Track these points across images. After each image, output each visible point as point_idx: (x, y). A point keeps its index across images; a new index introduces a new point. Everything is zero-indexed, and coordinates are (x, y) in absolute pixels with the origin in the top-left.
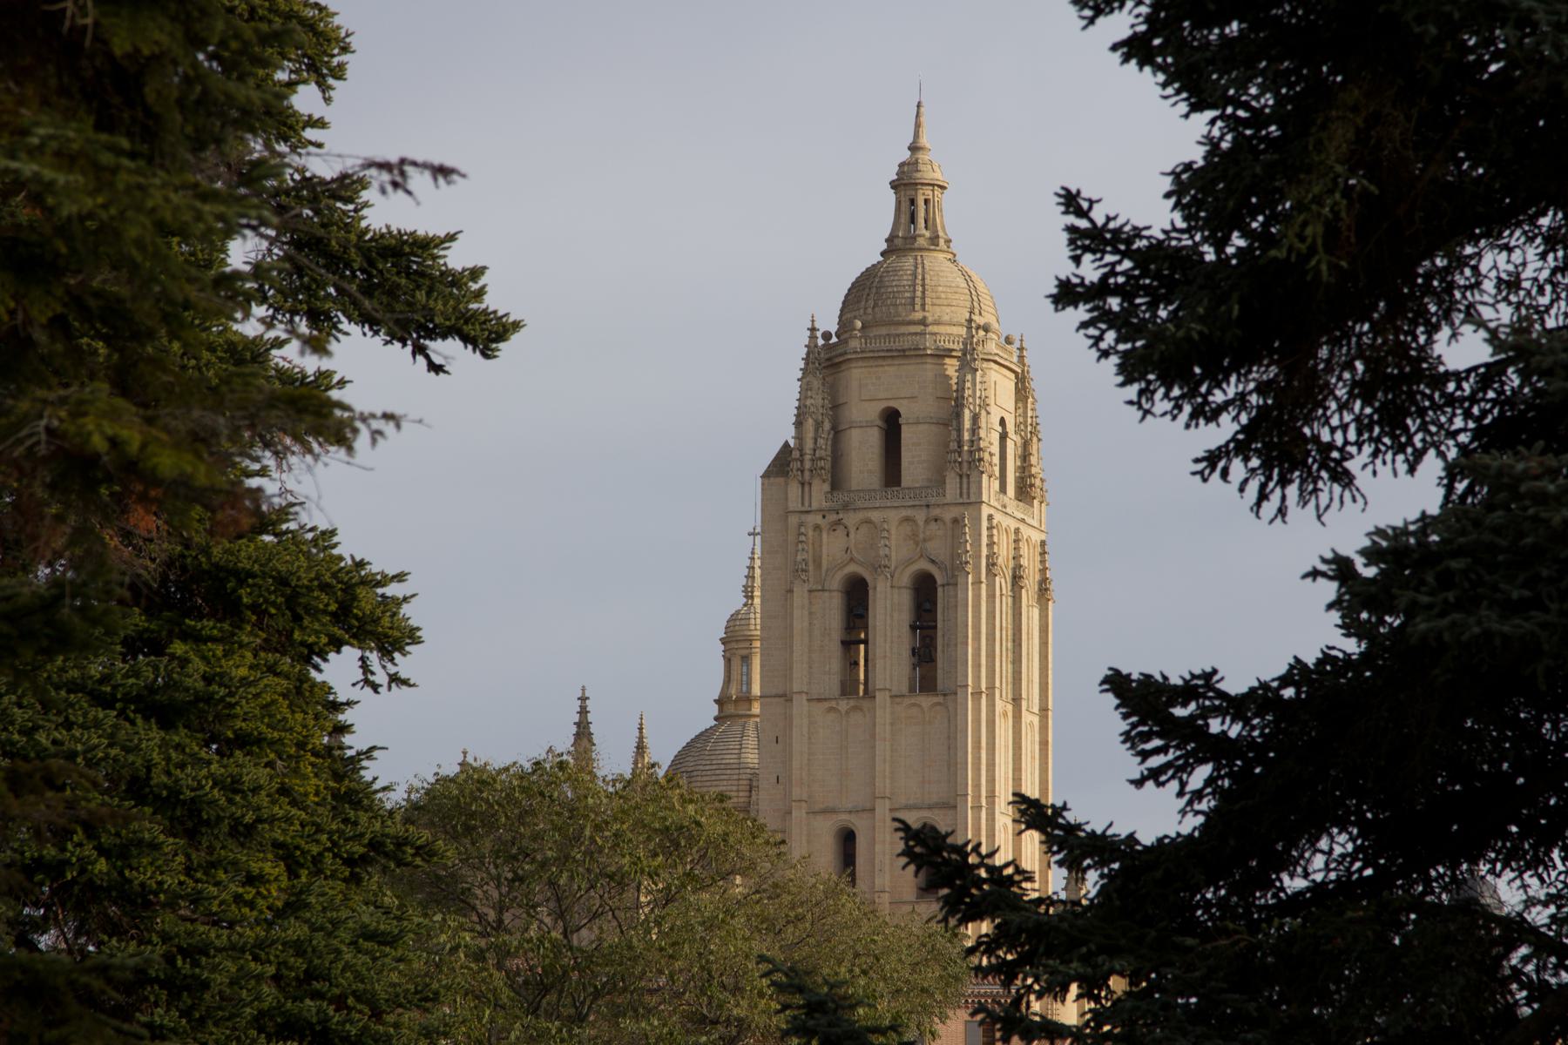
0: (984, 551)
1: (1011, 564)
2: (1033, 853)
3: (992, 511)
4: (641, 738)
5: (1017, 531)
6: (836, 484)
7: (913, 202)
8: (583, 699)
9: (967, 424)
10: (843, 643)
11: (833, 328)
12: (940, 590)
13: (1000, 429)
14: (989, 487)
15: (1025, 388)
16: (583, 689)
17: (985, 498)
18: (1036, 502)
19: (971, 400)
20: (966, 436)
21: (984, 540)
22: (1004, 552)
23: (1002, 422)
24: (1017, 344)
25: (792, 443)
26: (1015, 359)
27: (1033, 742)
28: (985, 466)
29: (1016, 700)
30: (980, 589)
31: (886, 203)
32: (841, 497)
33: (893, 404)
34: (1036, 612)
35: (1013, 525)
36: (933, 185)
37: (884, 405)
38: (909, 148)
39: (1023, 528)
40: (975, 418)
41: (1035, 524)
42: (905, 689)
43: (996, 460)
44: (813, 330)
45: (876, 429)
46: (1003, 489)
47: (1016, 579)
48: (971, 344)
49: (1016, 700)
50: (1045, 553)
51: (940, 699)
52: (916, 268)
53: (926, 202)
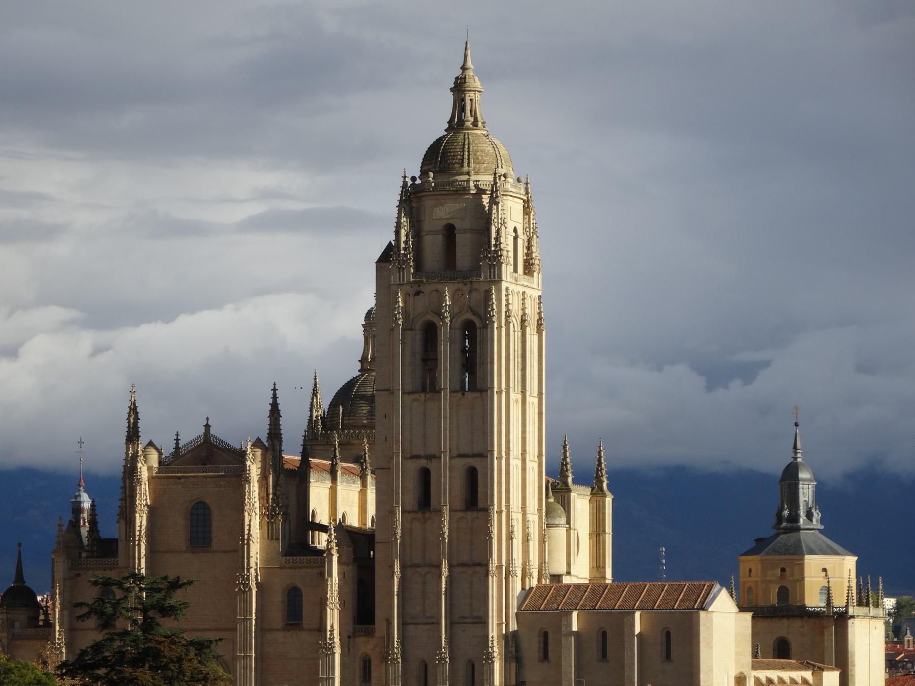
0: (504, 309)
1: (520, 313)
2: (534, 478)
3: (508, 285)
5: (524, 293)
7: (463, 100)
8: (275, 390)
9: (494, 235)
10: (422, 360)
11: (417, 174)
12: (478, 331)
13: (514, 234)
14: (507, 270)
15: (528, 207)
16: (275, 384)
17: (504, 278)
18: (535, 274)
19: (496, 220)
20: (493, 242)
21: (504, 302)
22: (515, 308)
23: (515, 230)
25: (393, 243)
26: (523, 192)
27: (534, 413)
28: (504, 259)
29: (523, 392)
30: (501, 331)
31: (449, 98)
33: (452, 221)
34: (536, 338)
35: (521, 289)
36: (475, 91)
37: (445, 222)
38: (461, 68)
39: (527, 290)
40: (498, 232)
41: (535, 286)
42: (458, 387)
43: (511, 254)
44: (405, 177)
45: (441, 236)
46: (515, 270)
47: (523, 321)
48: (496, 188)
49: (523, 392)
50: (541, 303)
52: (465, 141)
53: (471, 100)
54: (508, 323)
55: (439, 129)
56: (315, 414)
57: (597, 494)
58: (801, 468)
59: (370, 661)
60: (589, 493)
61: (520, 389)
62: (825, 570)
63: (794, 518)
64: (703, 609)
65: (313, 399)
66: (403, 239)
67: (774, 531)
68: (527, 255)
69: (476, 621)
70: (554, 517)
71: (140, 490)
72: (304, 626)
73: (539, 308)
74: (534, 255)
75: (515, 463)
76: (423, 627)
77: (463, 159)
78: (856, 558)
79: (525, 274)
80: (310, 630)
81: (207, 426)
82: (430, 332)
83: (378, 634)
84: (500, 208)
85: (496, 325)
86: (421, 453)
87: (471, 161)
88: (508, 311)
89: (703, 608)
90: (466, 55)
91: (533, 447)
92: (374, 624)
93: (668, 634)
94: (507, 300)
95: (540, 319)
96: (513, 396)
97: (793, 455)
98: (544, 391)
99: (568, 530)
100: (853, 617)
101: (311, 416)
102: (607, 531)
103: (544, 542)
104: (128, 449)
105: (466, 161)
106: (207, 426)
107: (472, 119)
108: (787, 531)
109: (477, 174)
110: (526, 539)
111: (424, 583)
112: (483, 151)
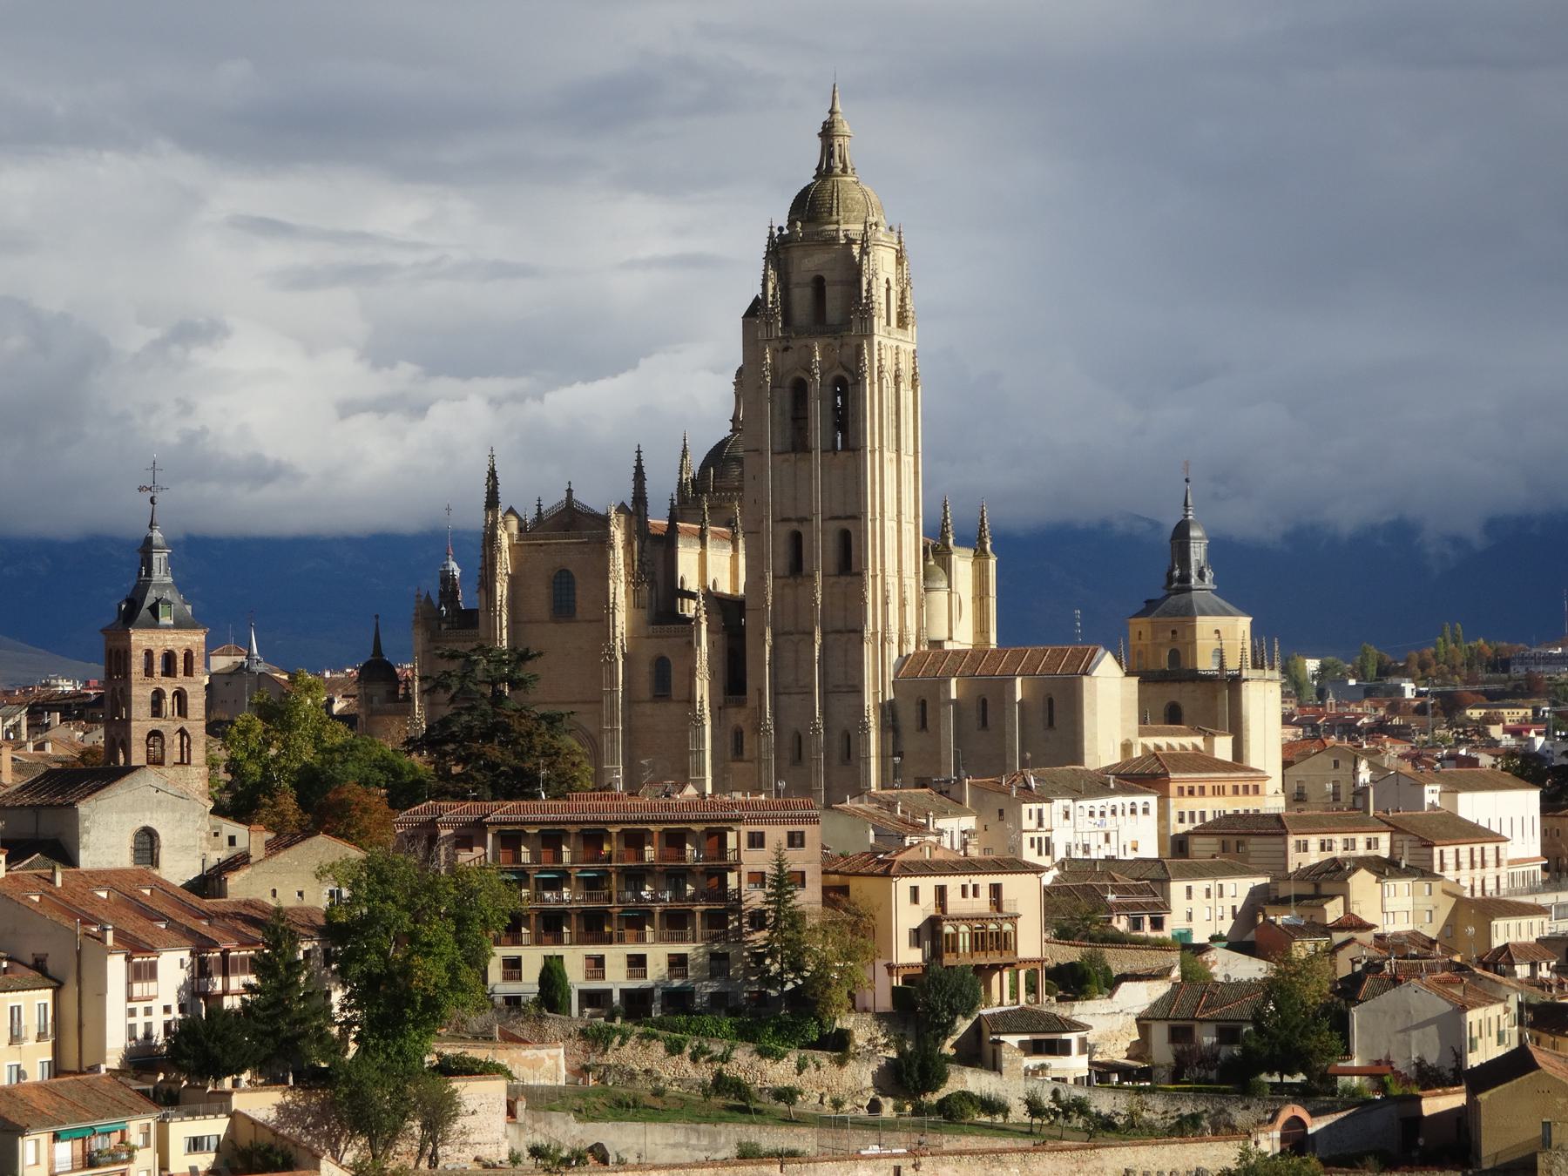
0: (876, 364)
1: (894, 368)
3: (880, 339)
4: (685, 445)
5: (897, 347)
7: (832, 145)
8: (639, 452)
9: (865, 287)
11: (785, 224)
13: (886, 286)
14: (879, 324)
15: (901, 257)
17: (876, 331)
18: (909, 327)
20: (864, 294)
21: (876, 357)
22: (888, 363)
23: (888, 281)
24: (896, 229)
25: (760, 296)
26: (895, 241)
28: (875, 312)
29: (898, 450)
31: (818, 143)
33: (819, 273)
34: (911, 394)
37: (814, 274)
39: (901, 344)
40: (869, 283)
41: (909, 340)
42: (829, 446)
43: (884, 306)
44: (771, 227)
46: (888, 323)
47: (897, 377)
49: (898, 450)
51: (851, 454)
53: (840, 145)
54: (880, 379)
55: (807, 177)
56: (685, 477)
57: (980, 555)
58: (1192, 526)
59: (742, 733)
60: (972, 555)
61: (895, 448)
62: (1217, 632)
63: (1185, 578)
64: (1086, 674)
65: (682, 461)
66: (770, 292)
67: (1165, 592)
68: (901, 307)
69: (850, 689)
70: (934, 581)
71: (501, 558)
72: (674, 698)
73: (914, 363)
74: (908, 308)
75: (890, 525)
76: (795, 696)
77: (831, 208)
78: (1250, 619)
79: (899, 327)
80: (679, 702)
81: (569, 491)
82: (800, 391)
84: (871, 258)
85: (868, 381)
86: (792, 516)
87: (841, 209)
88: (880, 366)
89: (1086, 673)
90: (834, 99)
91: (910, 508)
92: (744, 693)
93: (1051, 701)
94: (880, 355)
95: (915, 374)
96: (886, 455)
97: (1184, 512)
98: (920, 450)
100: (1247, 680)
101: (681, 479)
102: (991, 594)
103: (922, 607)
104: (487, 516)
105: (835, 210)
106: (569, 491)
107: (841, 166)
108: (1179, 591)
109: (847, 222)
110: (903, 604)
111: (797, 651)
112: (852, 199)
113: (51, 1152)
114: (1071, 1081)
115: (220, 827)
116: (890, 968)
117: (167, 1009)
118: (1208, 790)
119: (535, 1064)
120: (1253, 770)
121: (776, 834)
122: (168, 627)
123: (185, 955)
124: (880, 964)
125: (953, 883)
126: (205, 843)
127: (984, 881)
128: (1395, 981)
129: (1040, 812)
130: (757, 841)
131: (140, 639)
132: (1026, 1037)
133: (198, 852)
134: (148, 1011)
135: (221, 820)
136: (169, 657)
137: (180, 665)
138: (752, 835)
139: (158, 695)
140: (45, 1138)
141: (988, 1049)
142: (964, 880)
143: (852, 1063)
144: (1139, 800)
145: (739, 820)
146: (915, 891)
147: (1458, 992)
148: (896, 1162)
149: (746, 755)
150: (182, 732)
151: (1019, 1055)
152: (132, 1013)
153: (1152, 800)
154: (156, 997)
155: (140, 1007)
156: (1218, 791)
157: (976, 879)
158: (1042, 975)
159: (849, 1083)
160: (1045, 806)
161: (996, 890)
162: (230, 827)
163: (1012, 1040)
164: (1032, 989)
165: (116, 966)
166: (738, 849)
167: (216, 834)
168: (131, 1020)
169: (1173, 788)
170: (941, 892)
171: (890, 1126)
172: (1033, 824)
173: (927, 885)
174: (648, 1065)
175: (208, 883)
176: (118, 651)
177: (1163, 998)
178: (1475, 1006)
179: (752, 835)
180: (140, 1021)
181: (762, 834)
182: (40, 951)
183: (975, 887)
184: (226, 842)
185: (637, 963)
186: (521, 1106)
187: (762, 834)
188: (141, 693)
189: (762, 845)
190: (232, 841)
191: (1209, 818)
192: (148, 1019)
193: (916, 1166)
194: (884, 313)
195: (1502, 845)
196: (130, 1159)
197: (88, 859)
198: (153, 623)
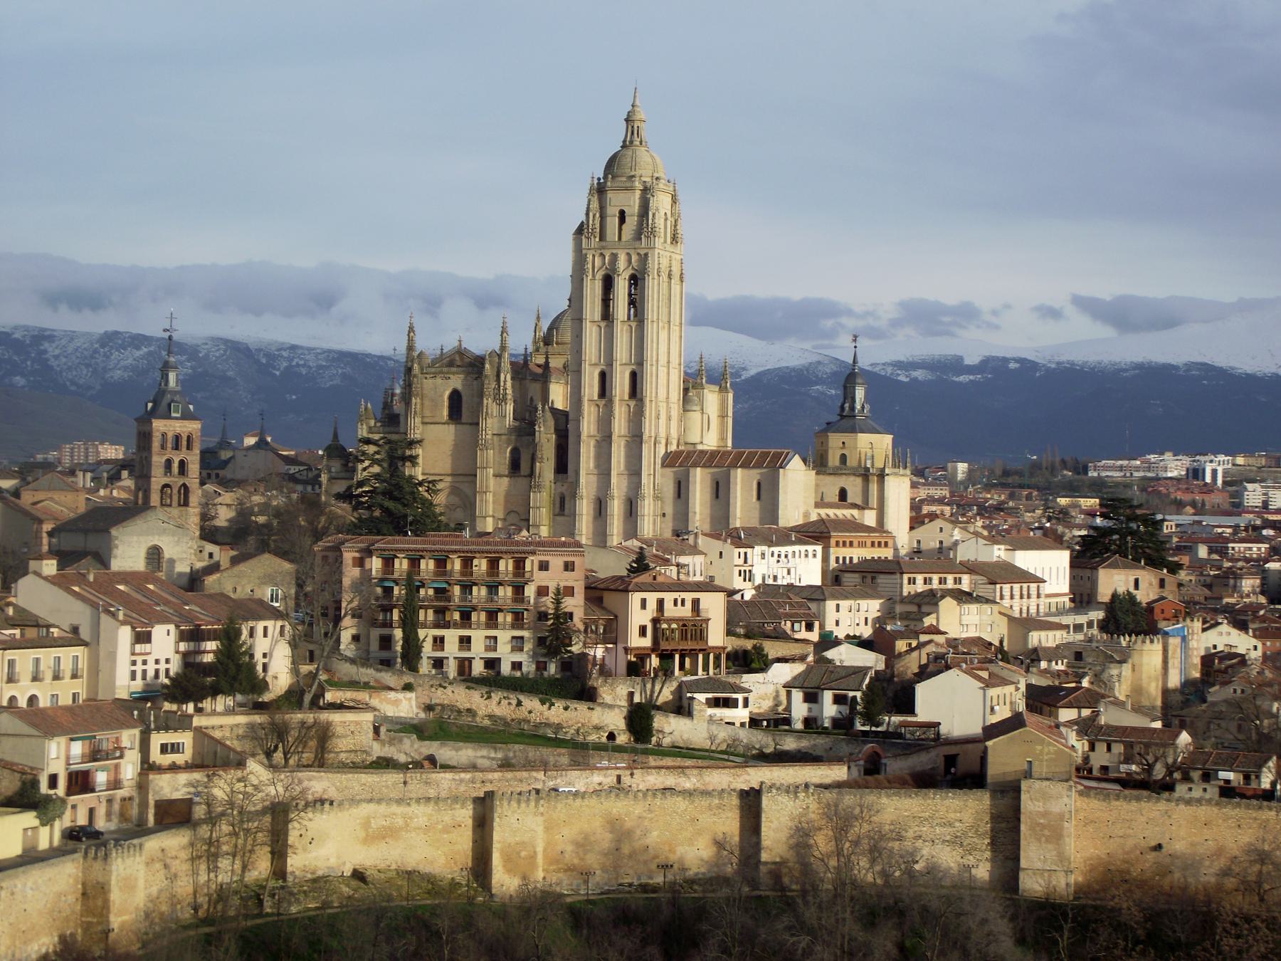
6: (602, 237)
11: (601, 176)
14: (659, 242)
21: (656, 262)
26: (672, 189)
29: (669, 322)
32: (603, 244)
34: (678, 287)
35: (668, 254)
40: (654, 215)
43: (662, 231)
46: (665, 242)
47: (670, 276)
57: (723, 390)
63: (852, 408)
82: (608, 283)
83: (570, 480)
90: (635, 97)
92: (566, 473)
99: (703, 413)
110: (669, 418)
113: (68, 749)
114: (738, 724)
115: (203, 547)
116: (626, 650)
117: (157, 662)
118: (855, 543)
119: (396, 703)
120: (885, 532)
121: (556, 562)
122: (176, 418)
123: (172, 627)
124: (620, 646)
125: (669, 597)
126: (193, 557)
127: (689, 597)
128: (948, 668)
129: (746, 553)
130: (544, 566)
131: (159, 425)
132: (710, 695)
133: (189, 562)
134: (145, 663)
135: (204, 543)
136: (177, 438)
137: (184, 443)
138: (541, 562)
139: (169, 463)
140: (63, 740)
141: (685, 703)
142: (676, 595)
143: (598, 709)
144: (810, 548)
145: (533, 553)
146: (644, 604)
147: (985, 674)
148: (618, 772)
149: (566, 511)
150: (184, 485)
151: (704, 707)
152: (134, 663)
153: (819, 549)
154: (150, 653)
155: (139, 659)
156: (862, 545)
157: (684, 595)
158: (723, 657)
159: (595, 721)
160: (749, 551)
161: (696, 603)
162: (210, 547)
163: (701, 697)
164: (717, 666)
165: (125, 634)
166: (532, 571)
167: (201, 551)
168: (133, 668)
169: (833, 542)
170: (661, 603)
171: (620, 749)
172: (741, 561)
173: (652, 598)
174: (468, 706)
175: (194, 582)
176: (144, 433)
177: (799, 675)
178: (994, 686)
179: (541, 562)
180: (139, 668)
181: (548, 562)
182: (76, 622)
183: (683, 601)
184: (207, 556)
185: (465, 642)
186: (383, 730)
187: (548, 562)
188: (158, 460)
189: (547, 569)
190: (211, 555)
191: (855, 561)
192: (144, 667)
193: (632, 775)
194: (662, 235)
195: (1041, 585)
196: (121, 757)
197: (116, 565)
198: (168, 417)
